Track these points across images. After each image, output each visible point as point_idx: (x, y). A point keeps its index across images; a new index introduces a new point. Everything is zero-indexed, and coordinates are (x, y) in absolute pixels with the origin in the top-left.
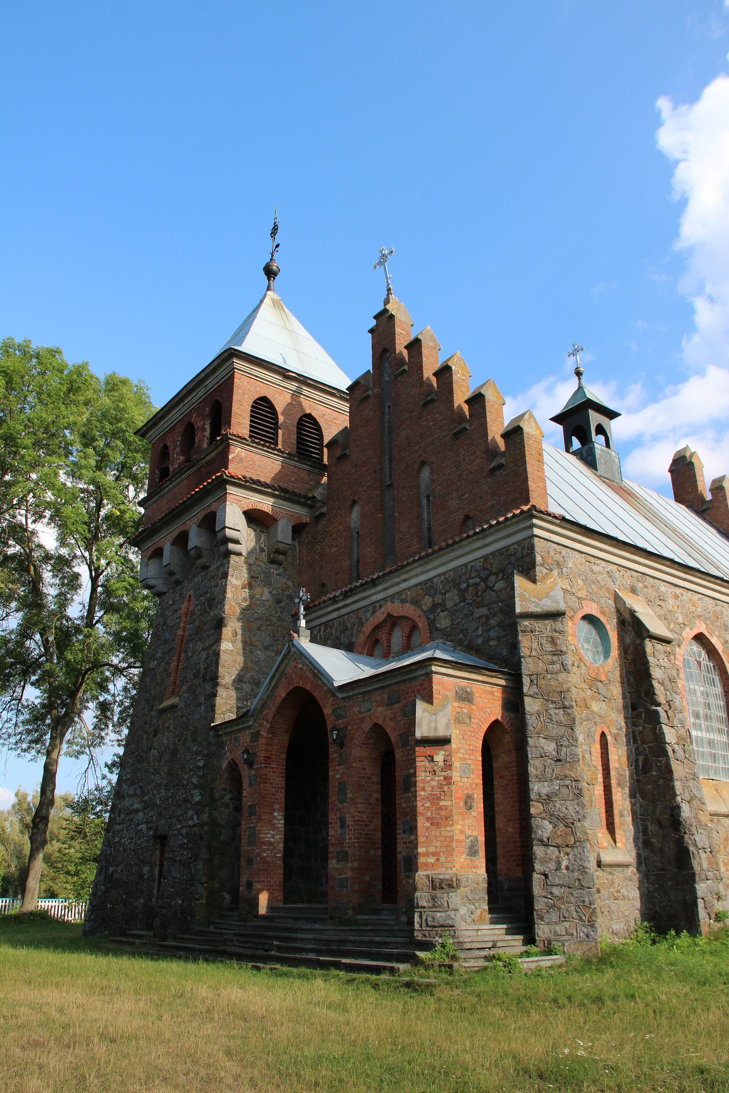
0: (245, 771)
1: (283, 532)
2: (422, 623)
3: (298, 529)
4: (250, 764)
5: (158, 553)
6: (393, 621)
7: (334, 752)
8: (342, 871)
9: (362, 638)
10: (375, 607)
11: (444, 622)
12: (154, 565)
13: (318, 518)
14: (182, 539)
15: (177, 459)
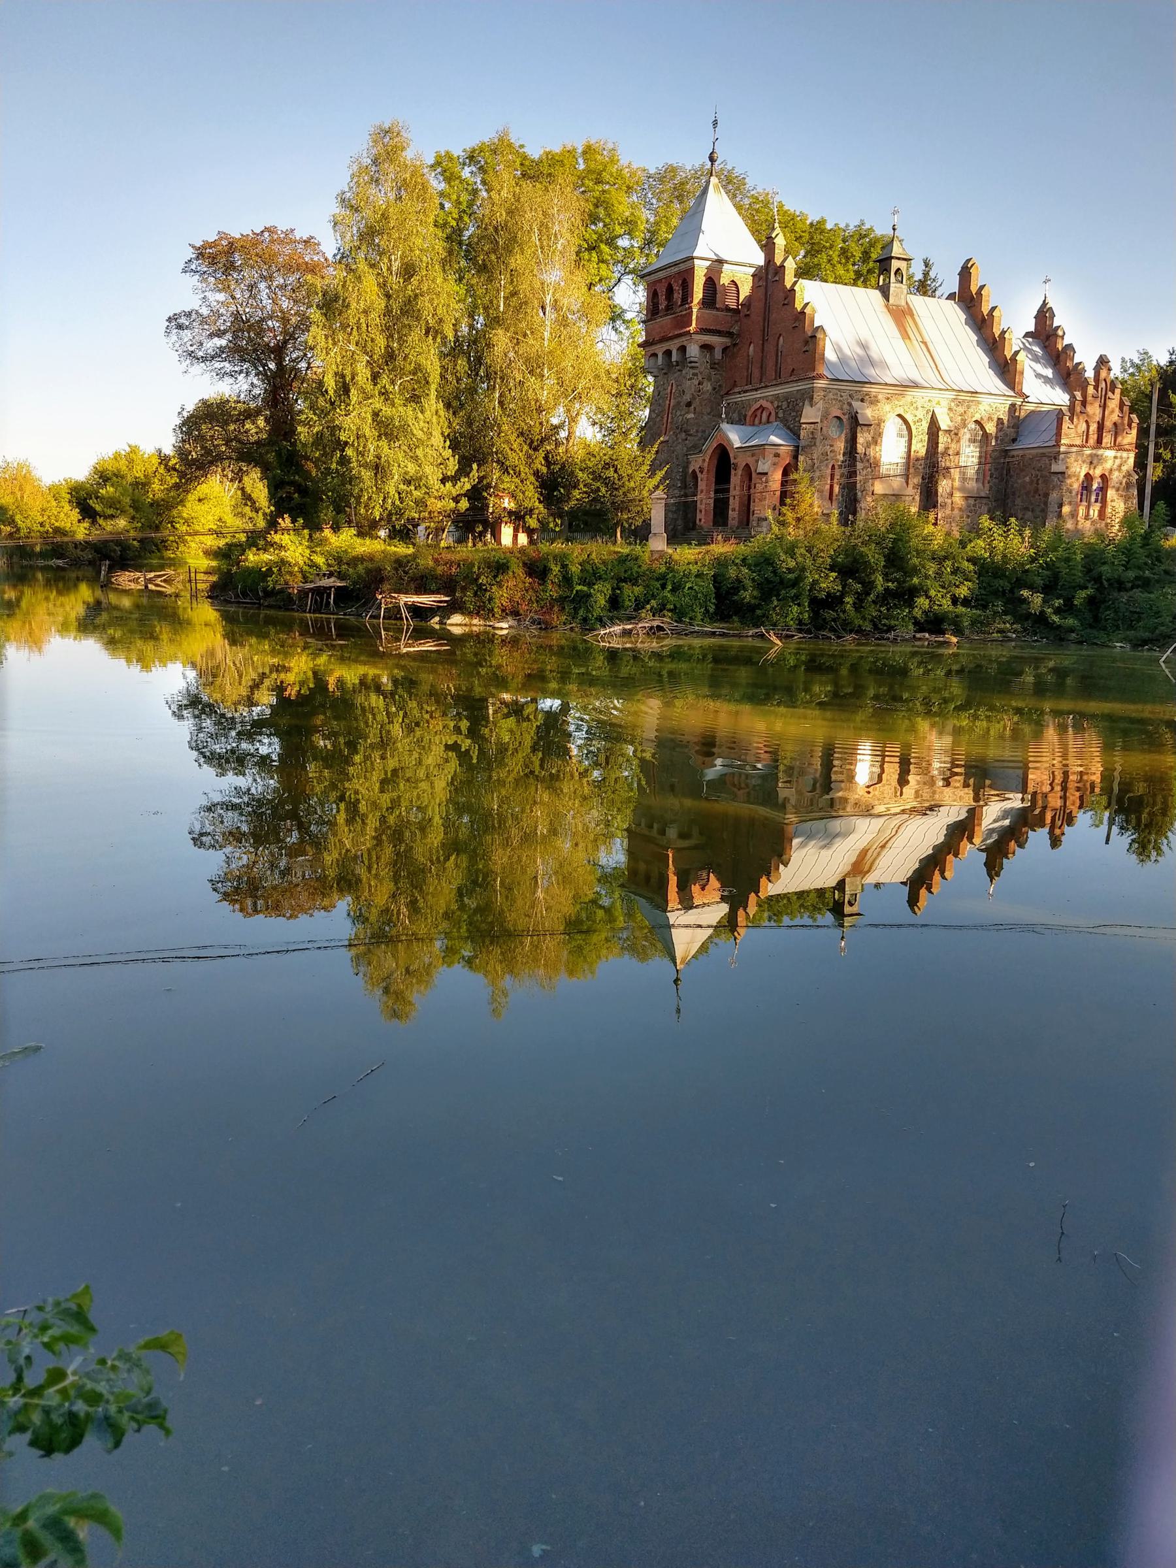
0: (699, 475)
1: (718, 354)
2: (773, 414)
3: (725, 350)
4: (702, 472)
5: (655, 355)
6: (762, 408)
7: (733, 472)
8: (733, 515)
9: (750, 413)
10: (756, 400)
11: (781, 415)
12: (652, 360)
13: (735, 345)
14: (668, 353)
15: (663, 305)
